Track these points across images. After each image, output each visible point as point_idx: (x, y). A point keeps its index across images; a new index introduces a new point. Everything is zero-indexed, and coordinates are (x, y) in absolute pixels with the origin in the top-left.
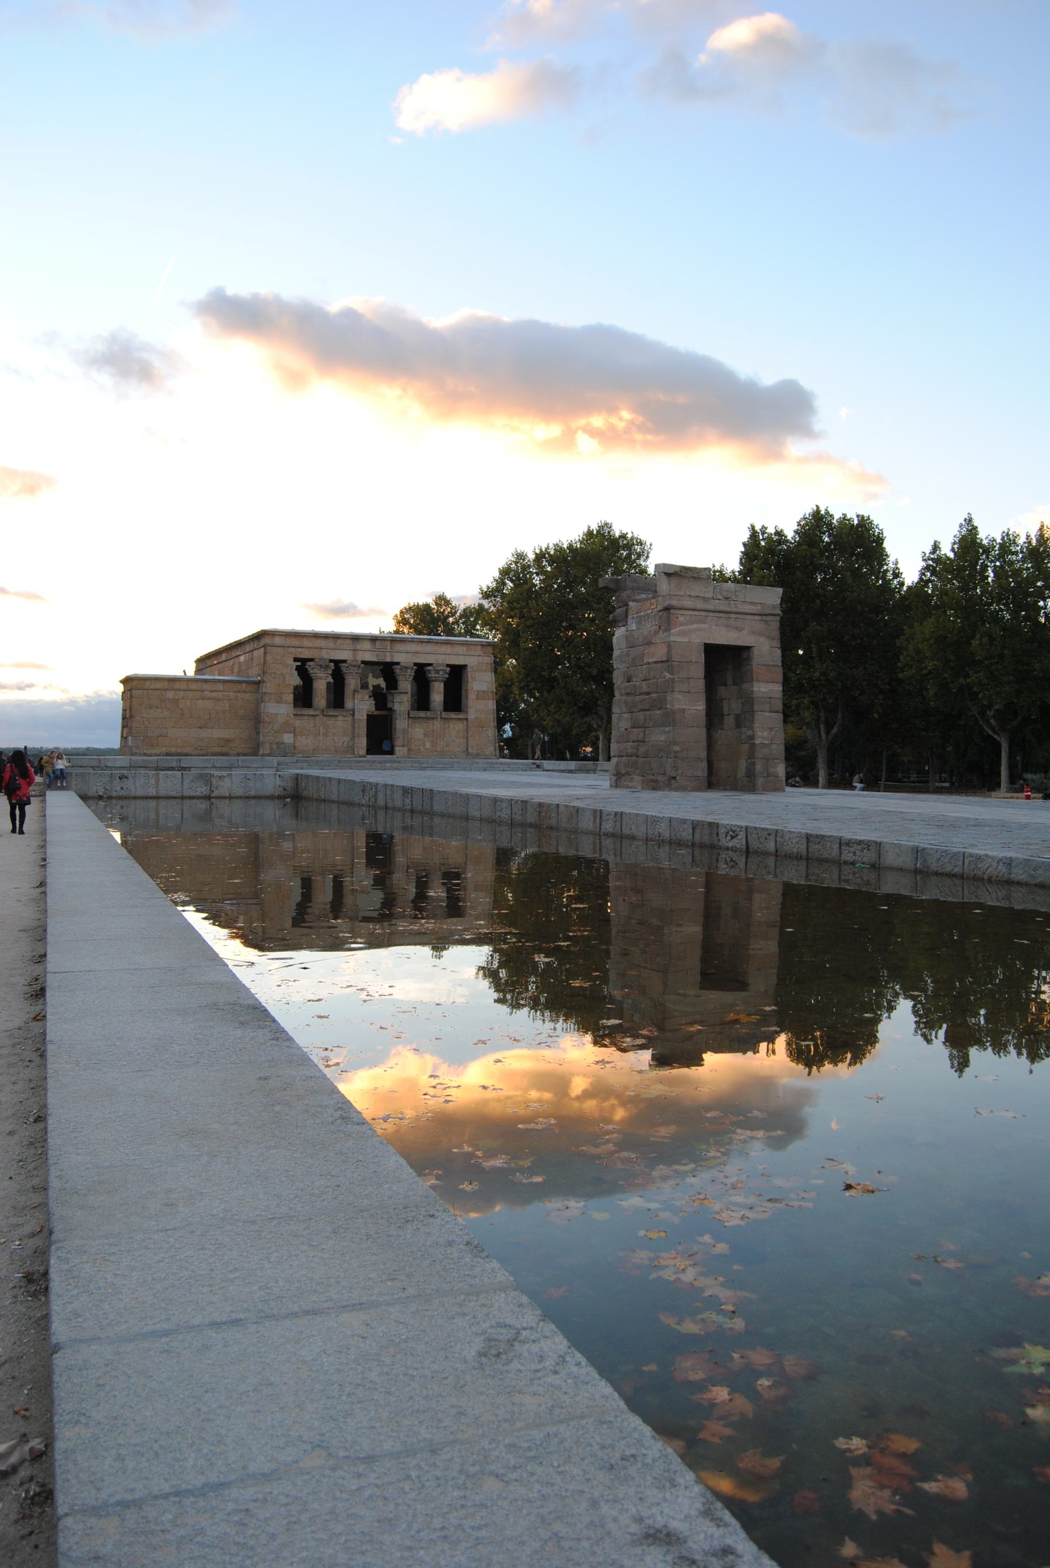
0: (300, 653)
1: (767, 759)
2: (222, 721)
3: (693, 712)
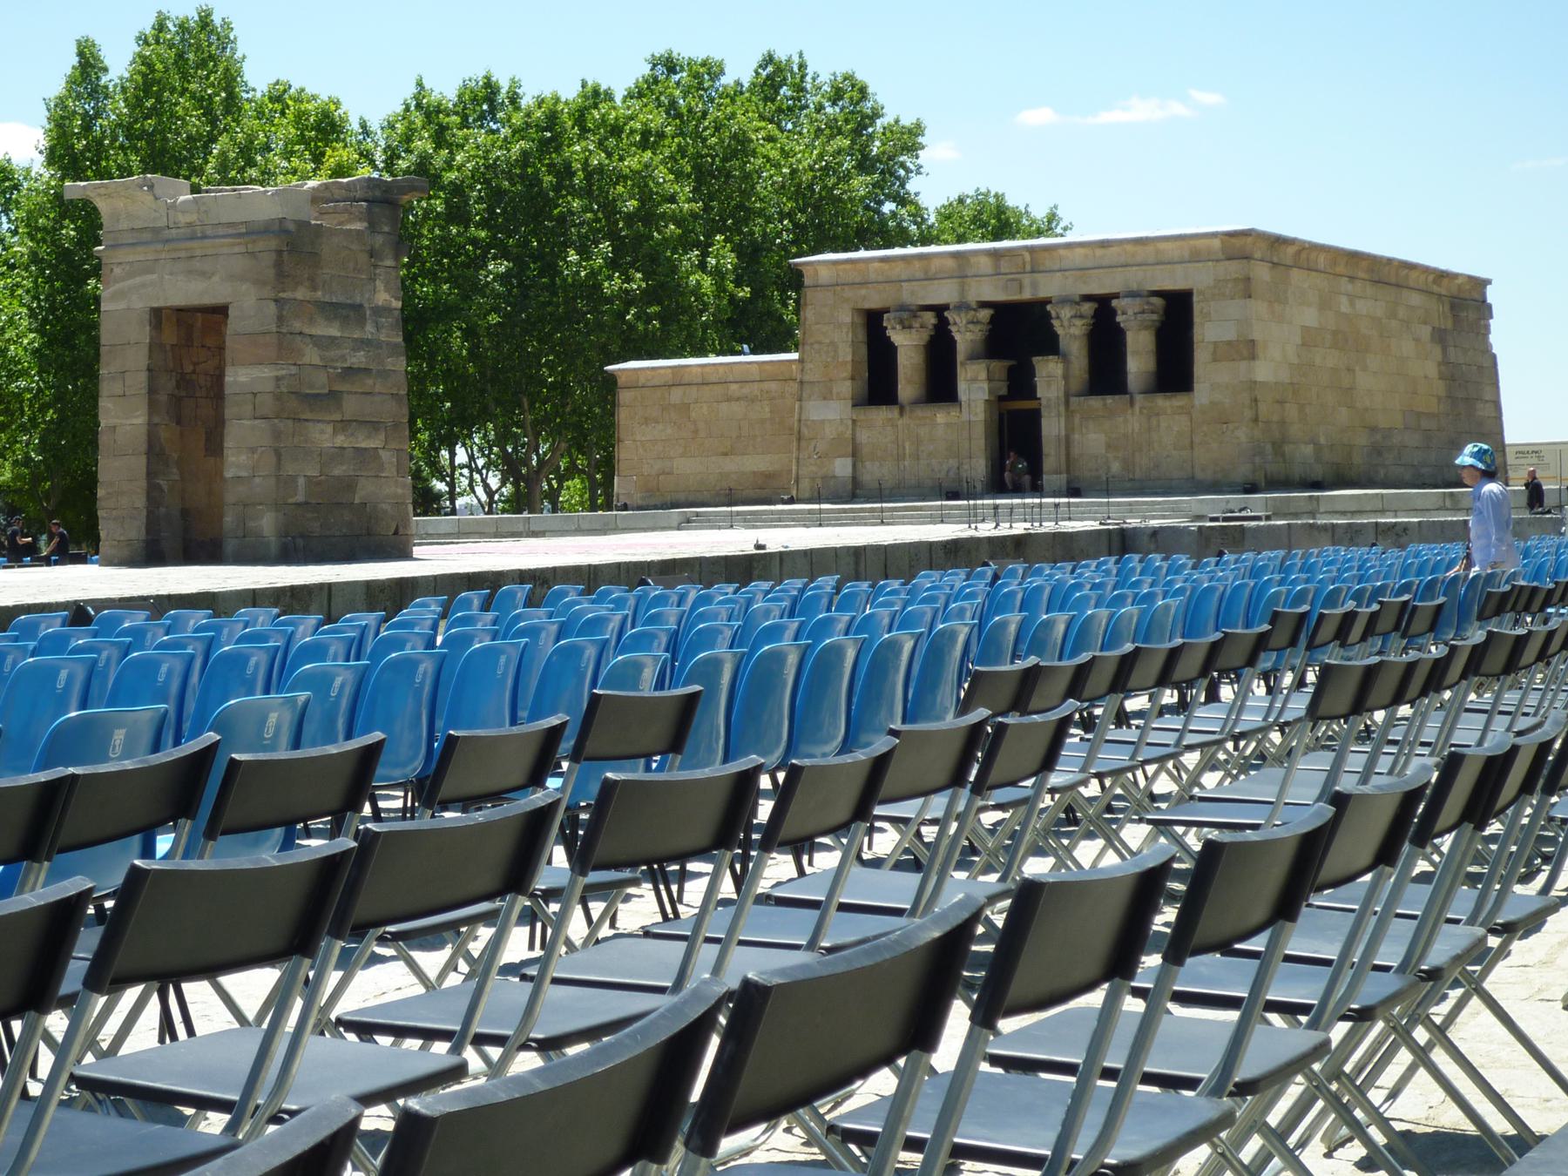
0: (864, 298)
1: (245, 505)
2: (759, 439)
3: (128, 428)
